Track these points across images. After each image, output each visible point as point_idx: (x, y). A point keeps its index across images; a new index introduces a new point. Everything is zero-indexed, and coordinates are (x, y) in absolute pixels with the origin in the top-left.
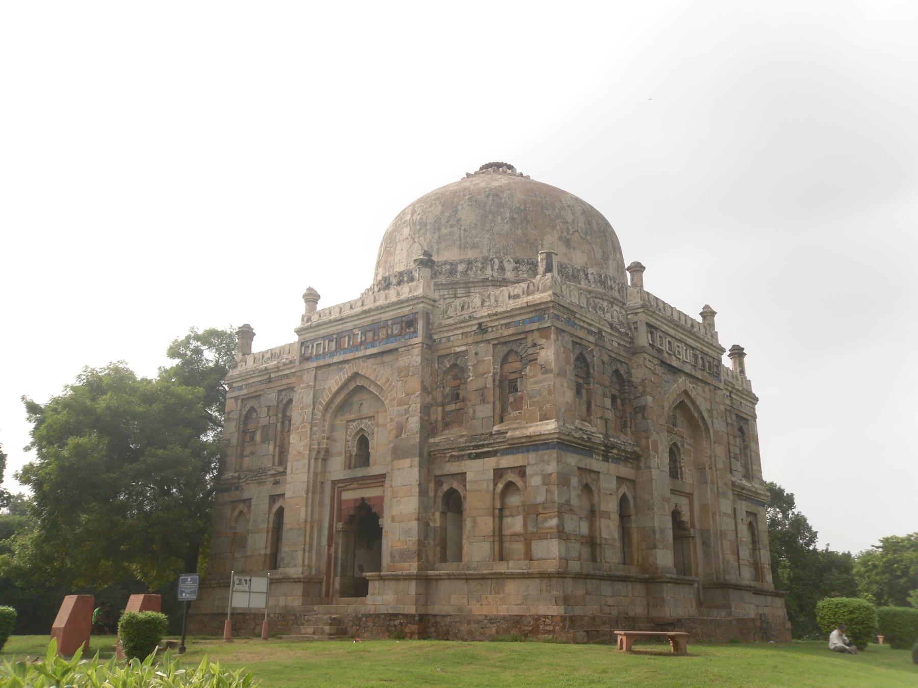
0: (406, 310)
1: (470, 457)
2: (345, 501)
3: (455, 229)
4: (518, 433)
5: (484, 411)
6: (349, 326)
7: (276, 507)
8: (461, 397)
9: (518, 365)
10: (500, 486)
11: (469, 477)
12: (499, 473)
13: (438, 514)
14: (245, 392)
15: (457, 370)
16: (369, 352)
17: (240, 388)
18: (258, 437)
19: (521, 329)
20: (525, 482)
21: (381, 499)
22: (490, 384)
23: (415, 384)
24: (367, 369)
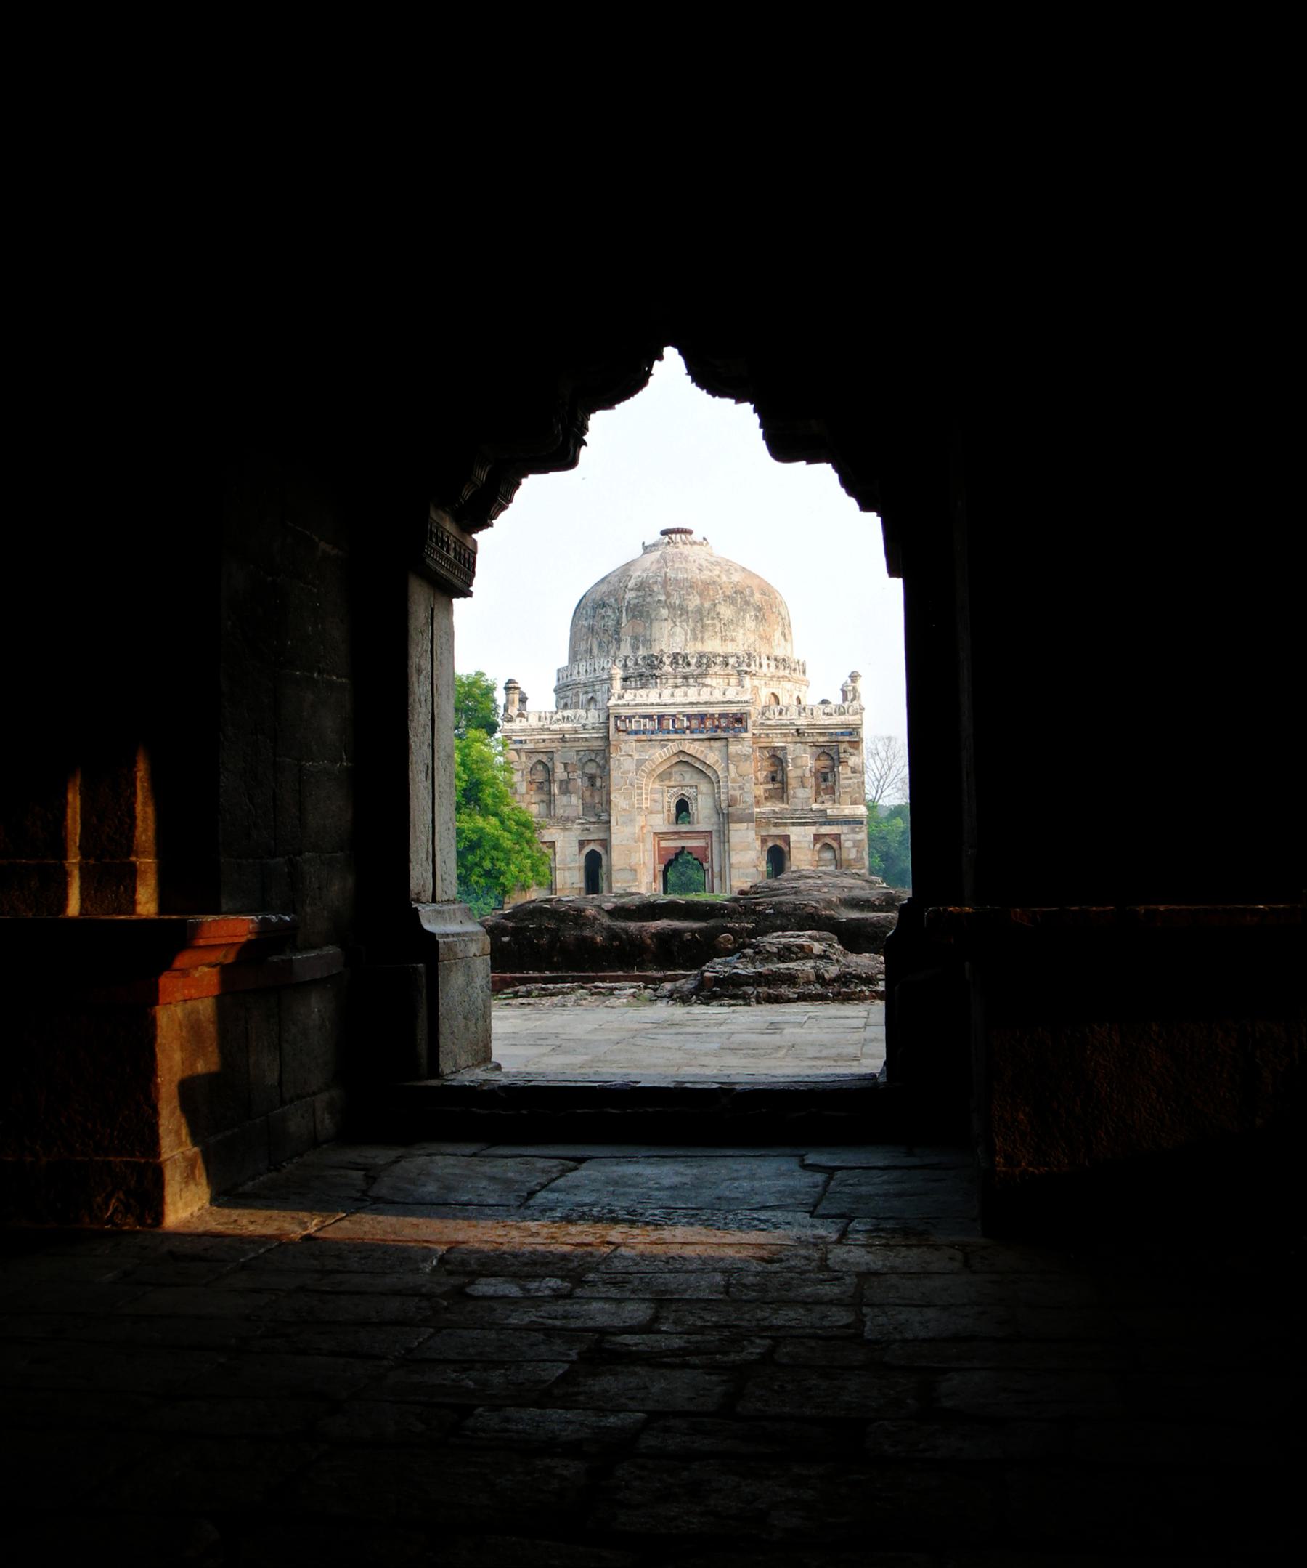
0: (734, 709)
1: (794, 824)
2: (665, 848)
3: (716, 622)
4: (836, 812)
5: (809, 792)
6: (673, 711)
7: (587, 850)
8: (779, 778)
9: (828, 763)
10: (818, 846)
11: (792, 839)
12: (817, 838)
13: (764, 863)
14: (529, 746)
15: (777, 761)
16: (695, 736)
17: (521, 742)
18: (555, 789)
19: (834, 738)
20: (840, 844)
21: (706, 849)
22: (808, 774)
23: (748, 768)
24: (694, 748)
